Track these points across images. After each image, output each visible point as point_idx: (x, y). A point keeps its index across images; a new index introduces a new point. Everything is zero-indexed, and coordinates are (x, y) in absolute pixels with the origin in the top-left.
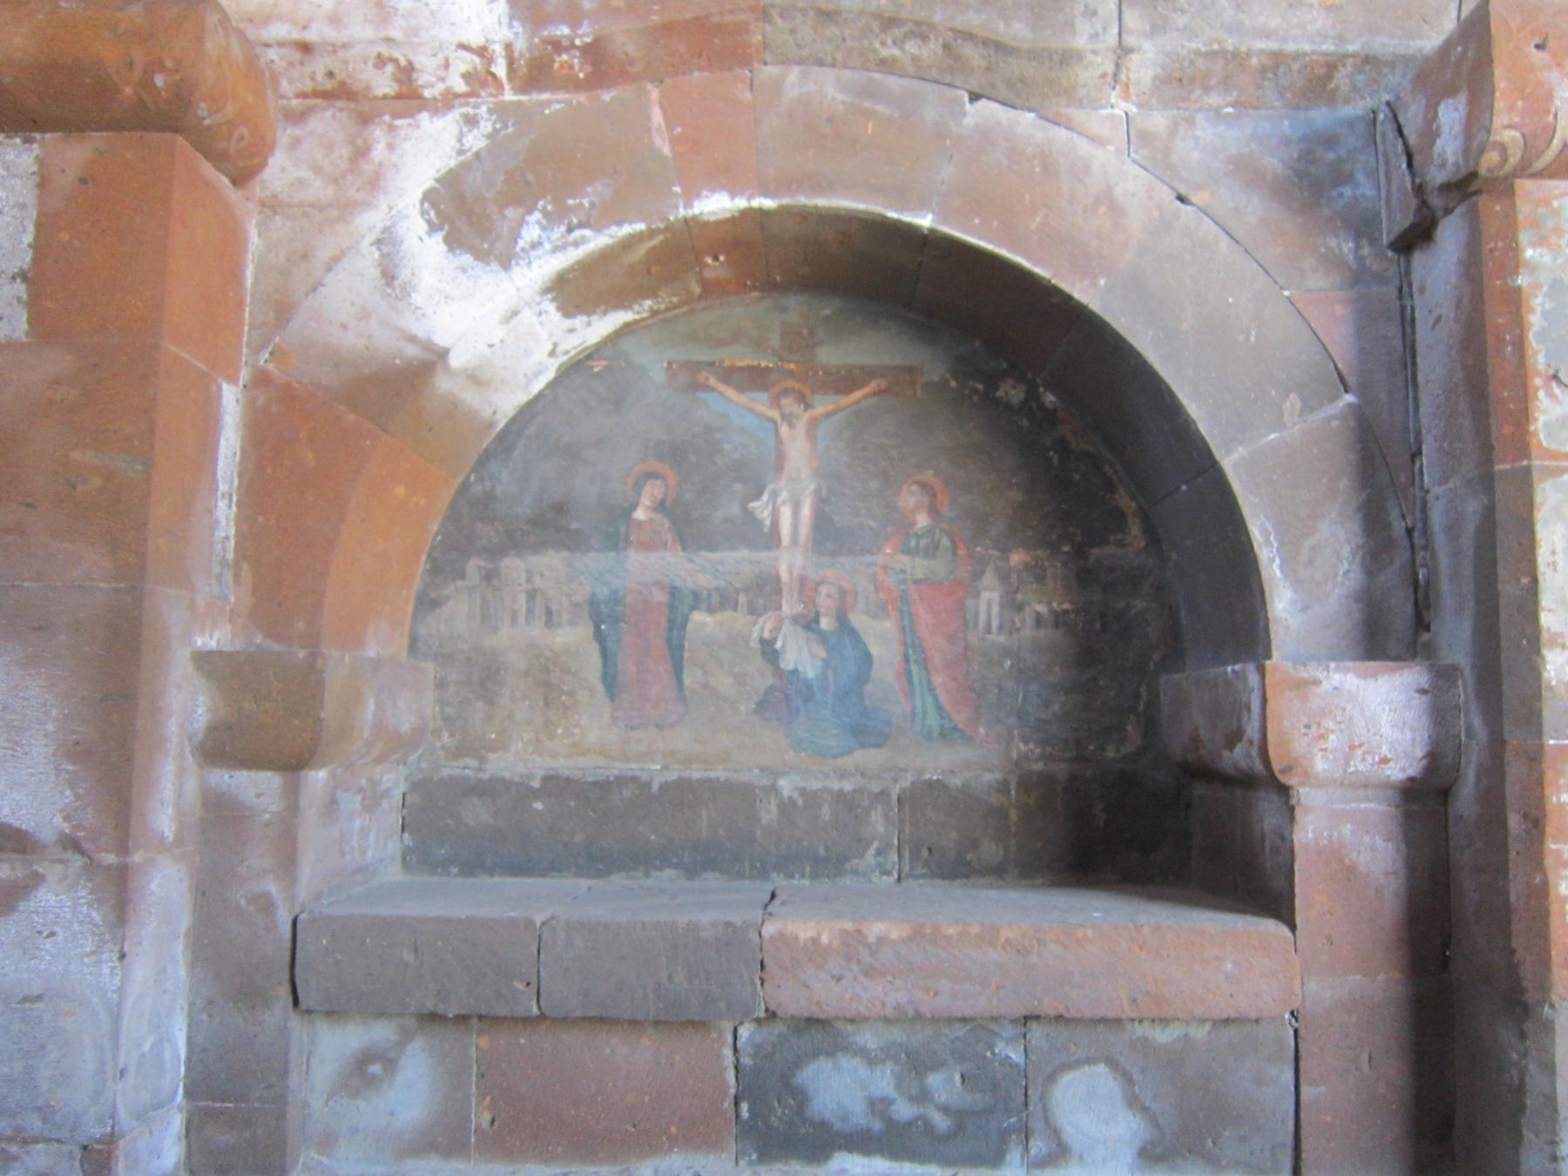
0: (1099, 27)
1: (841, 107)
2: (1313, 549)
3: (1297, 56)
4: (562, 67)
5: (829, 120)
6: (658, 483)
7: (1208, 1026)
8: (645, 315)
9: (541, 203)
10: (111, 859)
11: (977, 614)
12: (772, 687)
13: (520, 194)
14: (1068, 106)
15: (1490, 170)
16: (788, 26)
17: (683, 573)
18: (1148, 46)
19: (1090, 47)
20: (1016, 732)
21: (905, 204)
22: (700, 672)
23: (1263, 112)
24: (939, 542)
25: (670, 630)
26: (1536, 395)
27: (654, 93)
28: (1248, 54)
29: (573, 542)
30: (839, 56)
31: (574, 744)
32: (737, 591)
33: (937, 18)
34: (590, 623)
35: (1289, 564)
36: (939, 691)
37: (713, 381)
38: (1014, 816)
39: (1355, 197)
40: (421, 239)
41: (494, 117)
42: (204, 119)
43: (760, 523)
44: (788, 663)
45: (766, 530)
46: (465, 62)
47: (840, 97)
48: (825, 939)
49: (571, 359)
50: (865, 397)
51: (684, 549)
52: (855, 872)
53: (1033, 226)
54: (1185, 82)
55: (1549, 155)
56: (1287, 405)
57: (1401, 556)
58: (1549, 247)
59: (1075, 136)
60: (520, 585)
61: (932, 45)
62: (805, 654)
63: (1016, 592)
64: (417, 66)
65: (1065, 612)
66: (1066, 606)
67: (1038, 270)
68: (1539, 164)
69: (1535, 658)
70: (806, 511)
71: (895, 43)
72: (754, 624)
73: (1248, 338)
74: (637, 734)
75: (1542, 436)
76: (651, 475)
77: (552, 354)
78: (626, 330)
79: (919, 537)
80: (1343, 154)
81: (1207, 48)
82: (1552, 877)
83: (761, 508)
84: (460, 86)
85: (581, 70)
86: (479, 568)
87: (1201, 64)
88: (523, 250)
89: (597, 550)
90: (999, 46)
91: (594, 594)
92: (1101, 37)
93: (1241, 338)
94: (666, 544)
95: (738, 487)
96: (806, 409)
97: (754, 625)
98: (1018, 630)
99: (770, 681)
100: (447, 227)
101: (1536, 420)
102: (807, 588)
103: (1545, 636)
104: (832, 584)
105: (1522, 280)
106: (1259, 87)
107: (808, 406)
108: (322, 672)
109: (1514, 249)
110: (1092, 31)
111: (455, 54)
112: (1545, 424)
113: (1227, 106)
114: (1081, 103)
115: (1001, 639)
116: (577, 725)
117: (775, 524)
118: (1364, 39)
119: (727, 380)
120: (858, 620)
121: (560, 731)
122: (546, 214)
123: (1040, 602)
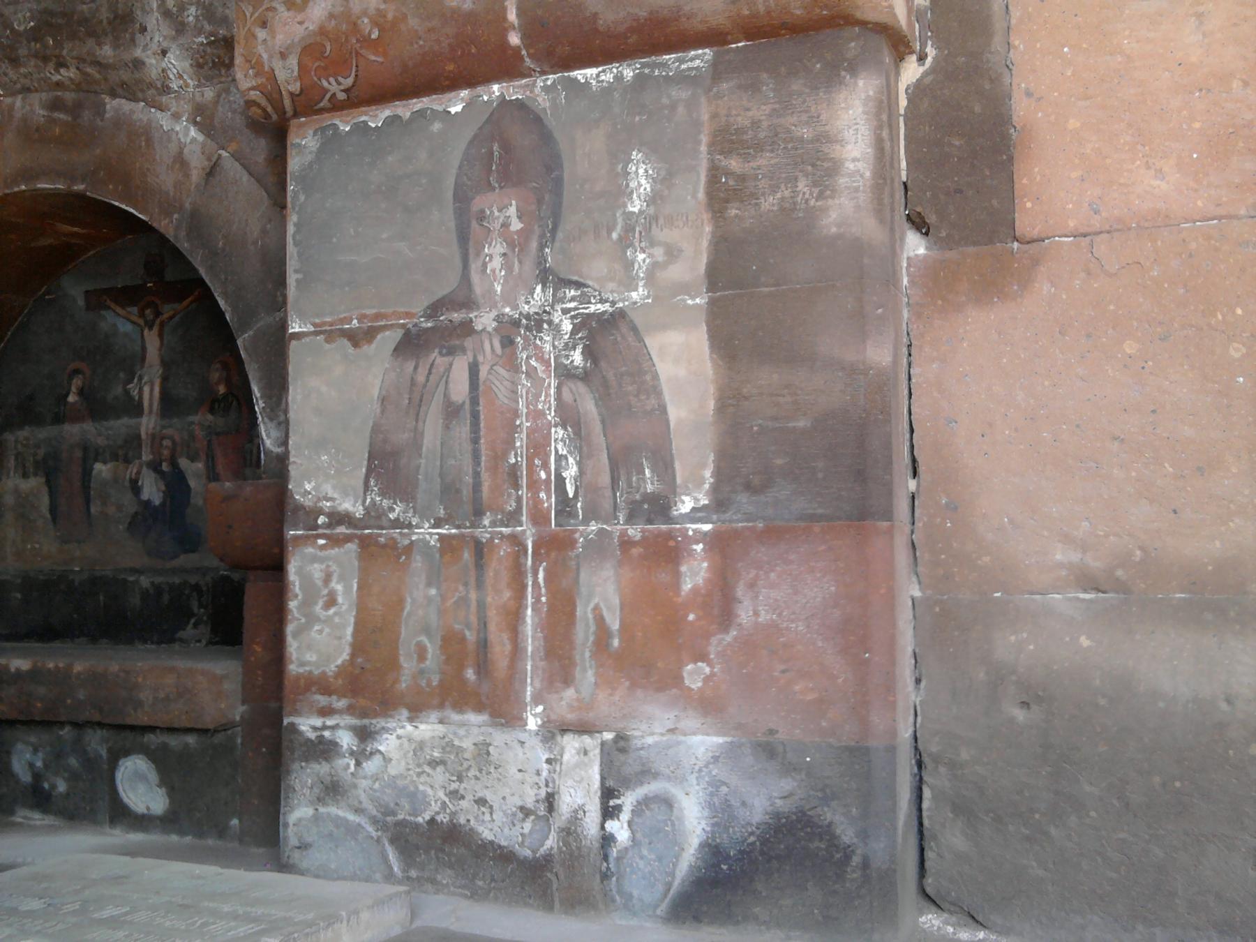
1: (42, 119)
5: (37, 130)
6: (80, 376)
37: (108, 302)
44: (145, 496)
45: (136, 403)
47: (42, 112)
50: (192, 302)
51: (93, 421)
52: (181, 640)
55: (287, 103)
62: (154, 489)
67: (140, 216)
72: (127, 468)
76: (76, 372)
83: (133, 388)
102: (156, 439)
104: (168, 438)
120: (183, 463)
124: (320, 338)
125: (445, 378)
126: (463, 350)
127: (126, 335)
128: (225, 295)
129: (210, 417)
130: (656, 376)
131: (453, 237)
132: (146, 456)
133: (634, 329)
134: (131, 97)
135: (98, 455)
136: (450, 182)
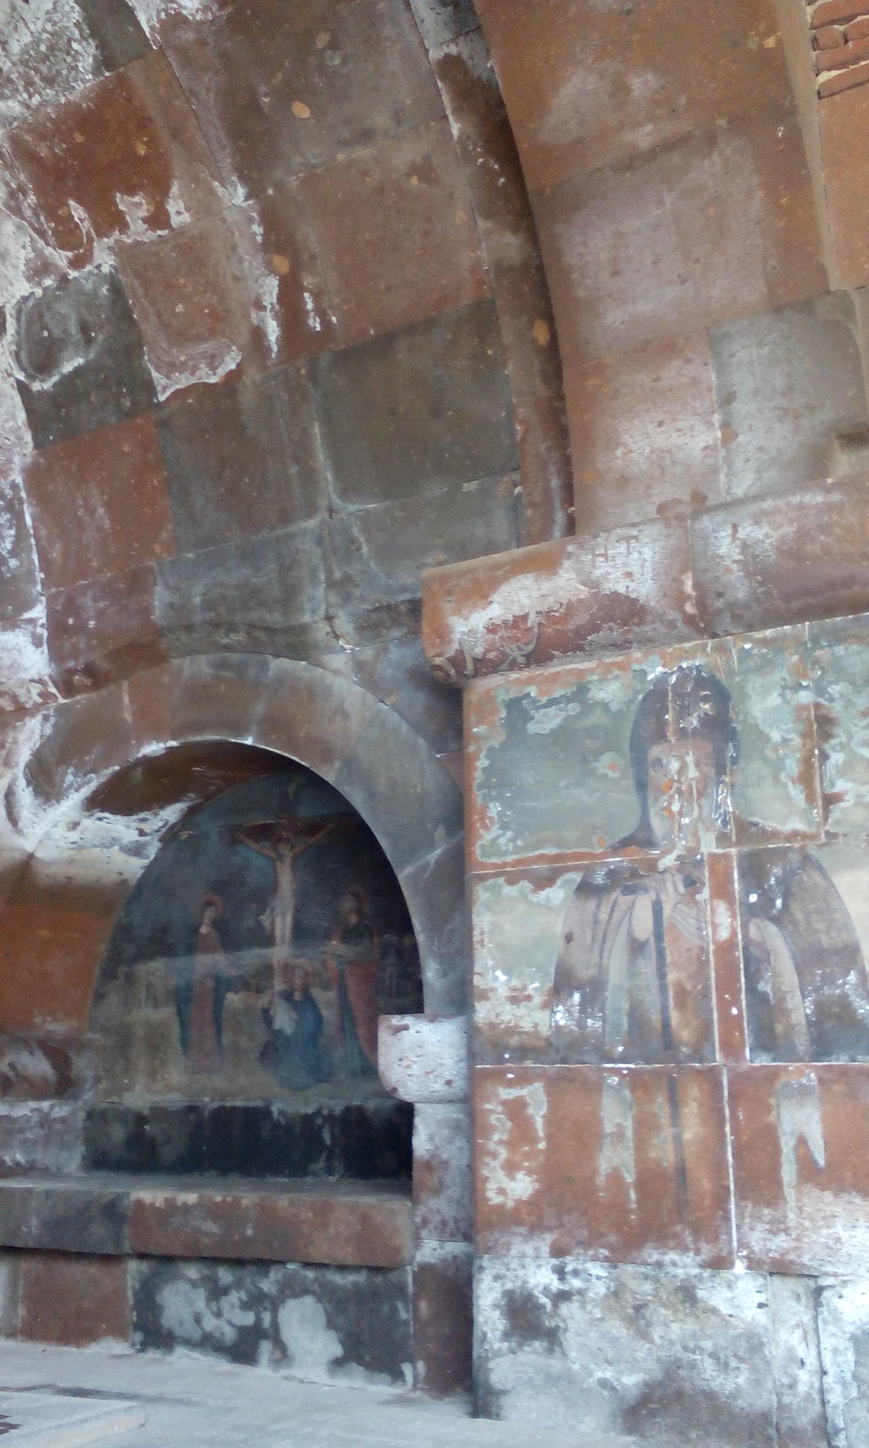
6: (213, 908)
28: (397, 605)
33: (237, 619)
46: (35, 689)
52: (314, 1174)
55: (470, 666)
67: (303, 763)
76: (209, 903)
83: (265, 919)
84: (39, 700)
95: (254, 906)
103: (476, 991)
116: (168, 1074)
117: (273, 928)
120: (316, 993)
124: (501, 880)
125: (627, 917)
126: (646, 890)
130: (846, 914)
131: (629, 783)
132: (278, 985)
133: (820, 869)
136: (627, 733)
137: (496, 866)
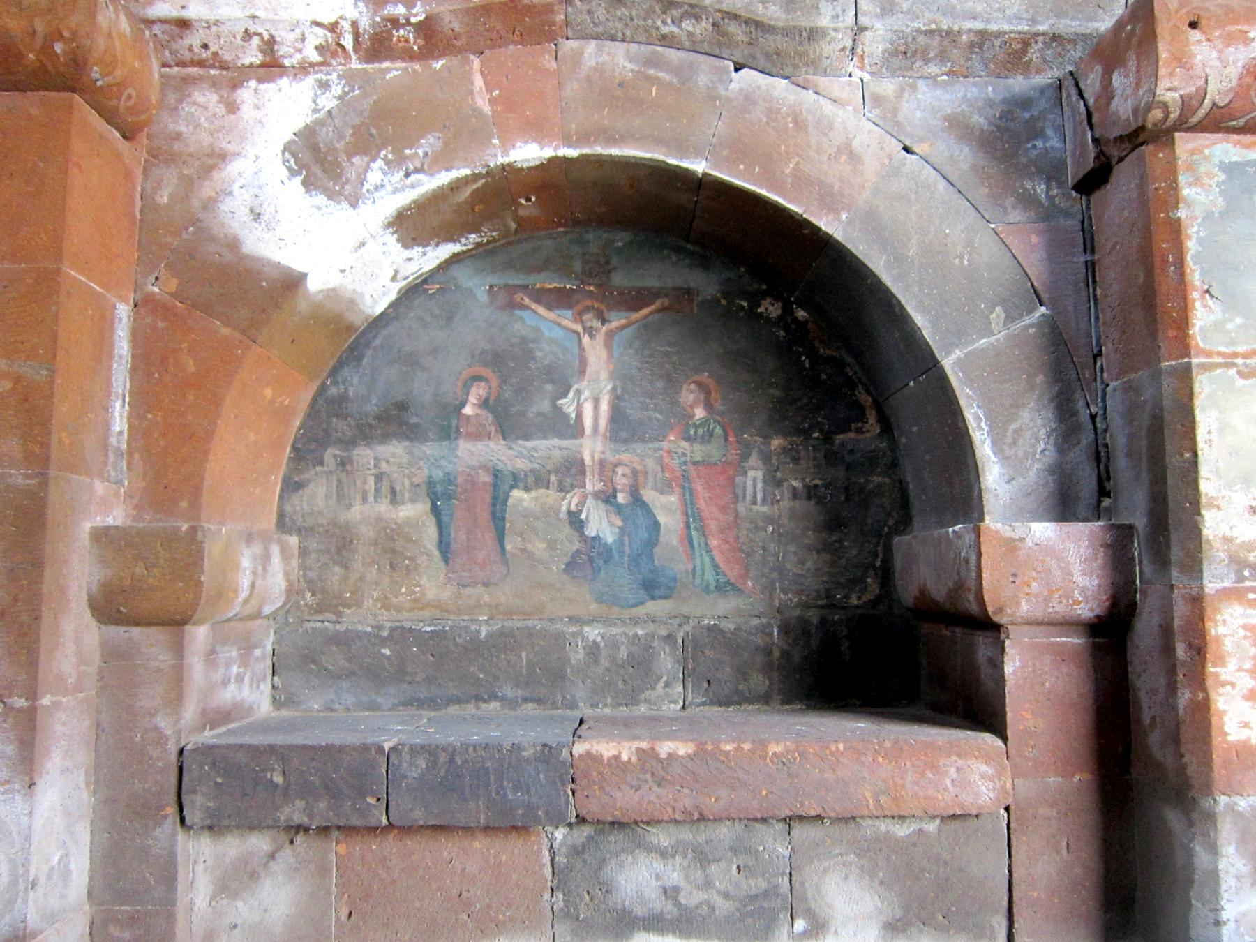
0: (839, 9)
2: (1016, 431)
3: (998, 34)
4: (399, 41)
5: (621, 85)
6: (483, 384)
7: (937, 821)
8: (470, 247)
9: (383, 153)
10: (21, 703)
11: (745, 487)
12: (578, 551)
13: (365, 144)
14: (814, 74)
15: (1155, 125)
16: (585, 7)
17: (504, 458)
18: (878, 25)
19: (832, 25)
20: (777, 585)
21: (682, 152)
22: (520, 539)
23: (971, 80)
24: (713, 430)
25: (494, 505)
26: (1194, 306)
27: (476, 63)
29: (412, 433)
30: (628, 33)
31: (416, 601)
32: (549, 473)
34: (428, 499)
35: (997, 444)
36: (715, 553)
37: (527, 301)
38: (777, 653)
39: (1045, 149)
40: (283, 182)
41: (343, 82)
42: (98, 80)
43: (567, 416)
44: (591, 531)
46: (318, 36)
47: (629, 66)
48: (625, 757)
49: (409, 283)
50: (651, 313)
51: (504, 439)
53: (787, 171)
54: (908, 55)
55: (1202, 112)
56: (994, 315)
57: (1086, 438)
58: (1202, 186)
59: (821, 98)
60: (369, 469)
61: (703, 24)
62: (605, 524)
63: (776, 471)
64: (278, 39)
65: (816, 486)
66: (817, 482)
68: (1194, 120)
69: (1196, 517)
70: (604, 406)
71: (673, 22)
72: (563, 499)
73: (961, 262)
74: (468, 591)
75: (1198, 338)
76: (477, 378)
77: (394, 279)
78: (455, 259)
79: (696, 427)
80: (1036, 113)
81: (927, 28)
82: (1213, 695)
83: (568, 405)
84: (315, 57)
85: (414, 44)
86: (335, 456)
87: (922, 40)
88: (368, 191)
89: (433, 440)
90: (758, 25)
91: (431, 477)
92: (840, 19)
93: (957, 261)
94: (490, 434)
95: (549, 387)
96: (603, 324)
97: (563, 500)
98: (778, 501)
99: (577, 545)
100: (304, 173)
101: (1194, 325)
102: (604, 468)
103: (1204, 500)
105: (1182, 213)
106: (968, 59)
107: (604, 321)
108: (202, 542)
109: (1174, 187)
110: (834, 13)
111: (310, 30)
112: (1201, 329)
113: (942, 74)
114: (825, 72)
115: (765, 509)
116: (418, 585)
118: (1051, 21)
119: (538, 301)
120: (648, 495)
121: (403, 590)
122: (385, 159)
123: (796, 479)
124: (1232, 372)
127: (552, 341)
128: (923, 310)
129: (685, 444)
132: (592, 484)
134: (768, 67)
135: (516, 480)
137: (1220, 354)
